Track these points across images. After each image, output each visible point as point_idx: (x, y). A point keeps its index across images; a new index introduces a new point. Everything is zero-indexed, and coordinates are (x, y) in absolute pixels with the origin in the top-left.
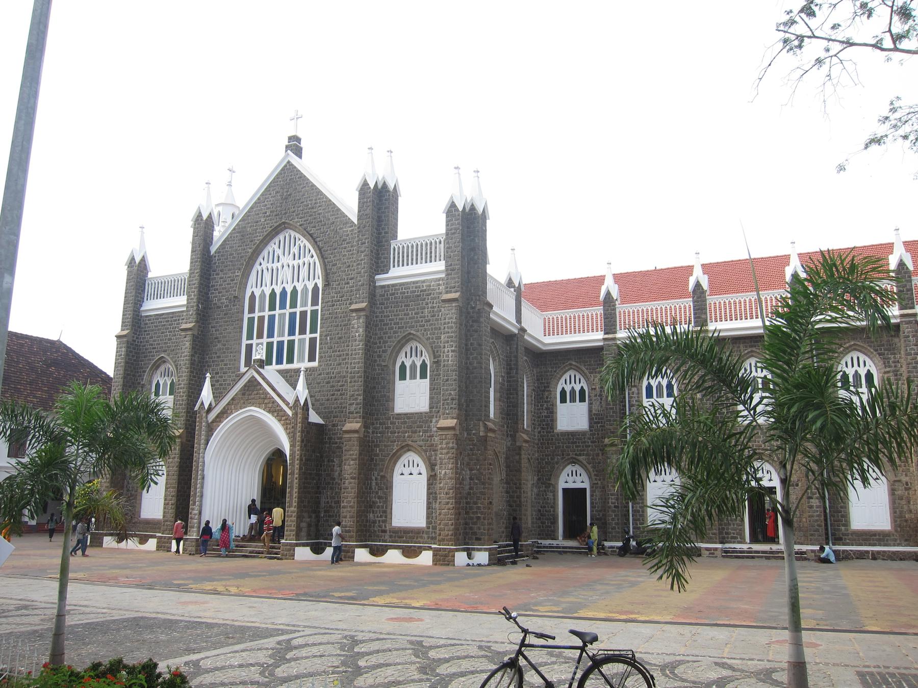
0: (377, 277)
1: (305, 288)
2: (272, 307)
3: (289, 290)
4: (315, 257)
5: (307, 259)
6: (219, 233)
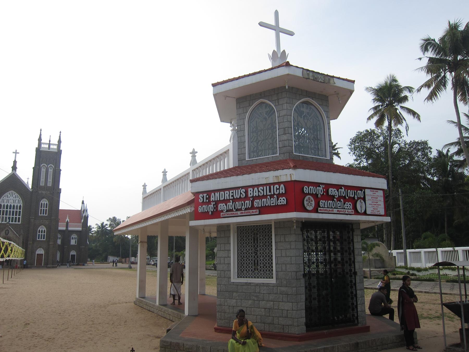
1: (17, 206)
5: (18, 199)
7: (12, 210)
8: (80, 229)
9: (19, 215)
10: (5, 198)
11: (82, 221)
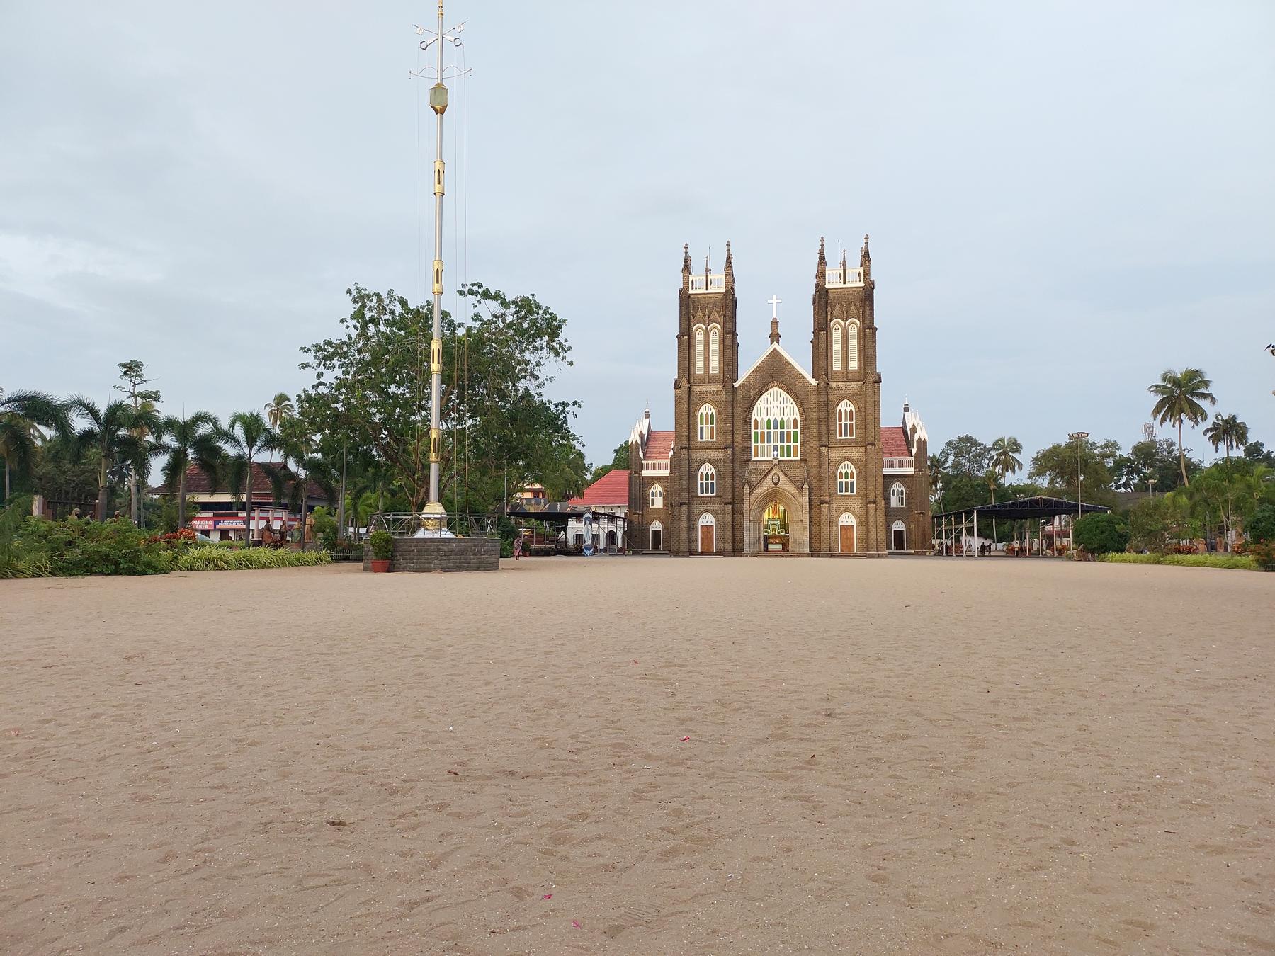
2: (769, 427)
7: (779, 430)
8: (911, 470)
9: (795, 441)
11: (914, 451)
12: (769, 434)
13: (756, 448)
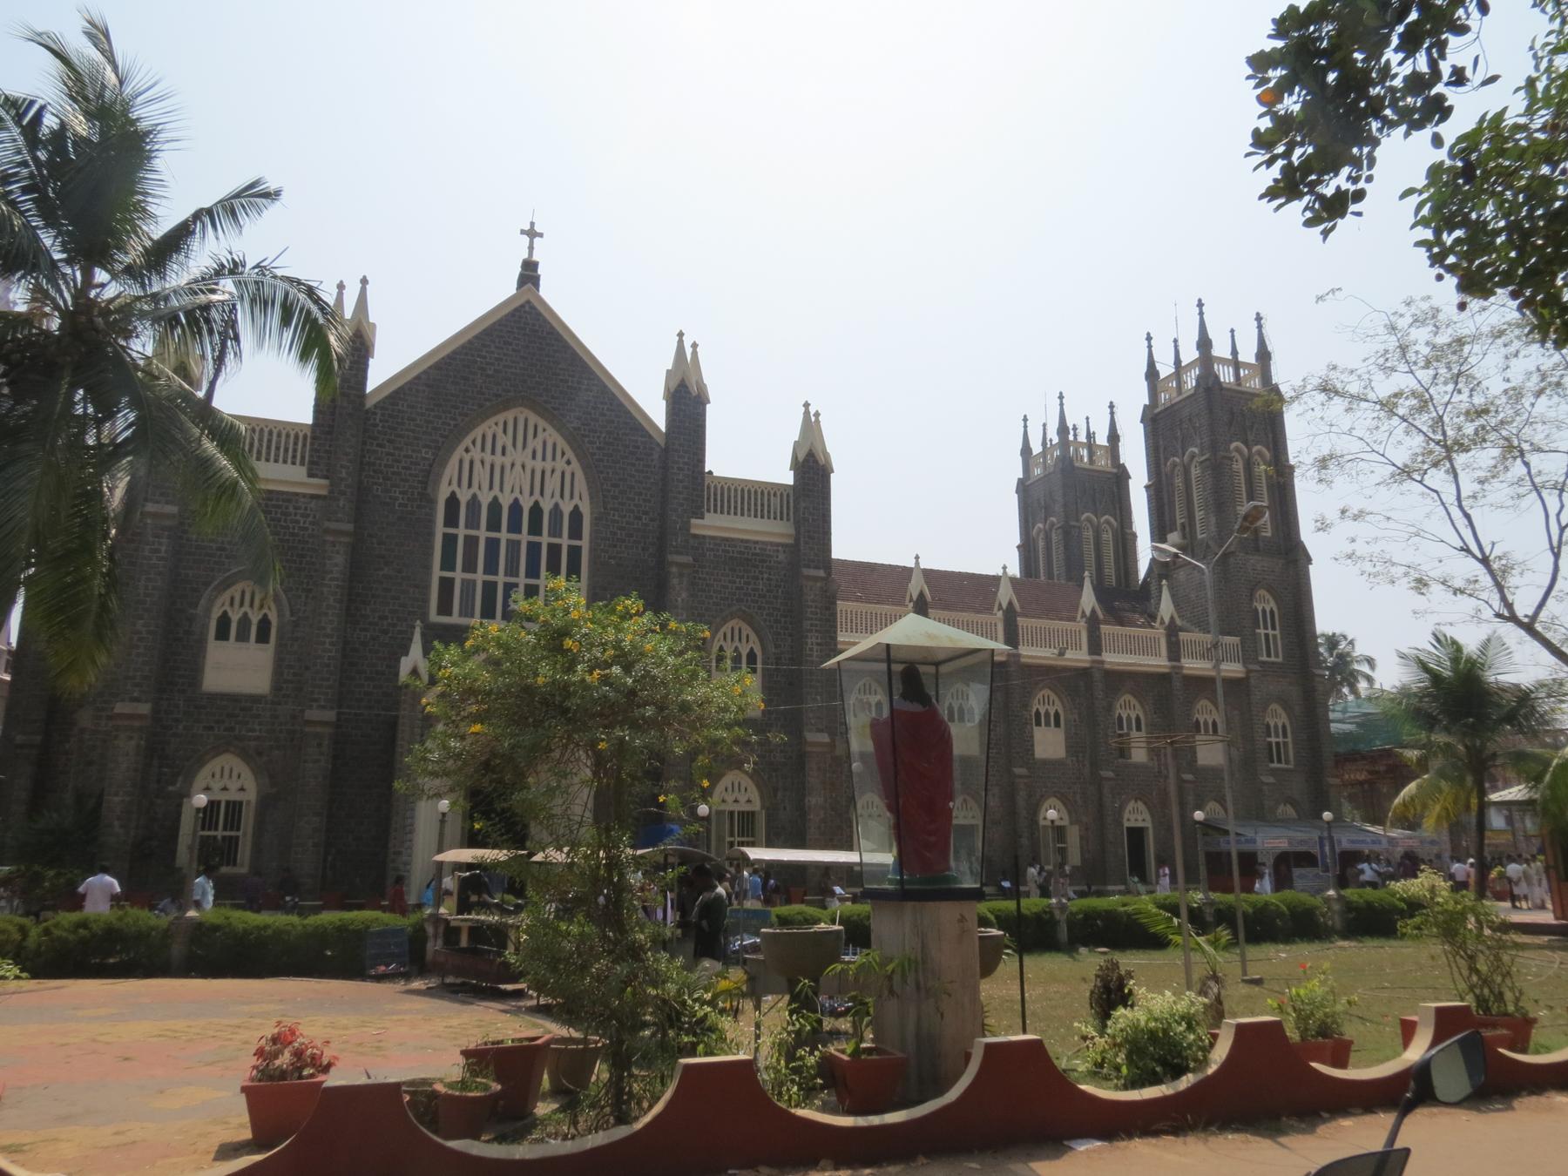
0: (693, 521)
1: (556, 512)
2: (494, 525)
3: (526, 505)
4: (575, 465)
6: (380, 372)
10: (476, 453)
12: (493, 545)
13: (447, 585)
